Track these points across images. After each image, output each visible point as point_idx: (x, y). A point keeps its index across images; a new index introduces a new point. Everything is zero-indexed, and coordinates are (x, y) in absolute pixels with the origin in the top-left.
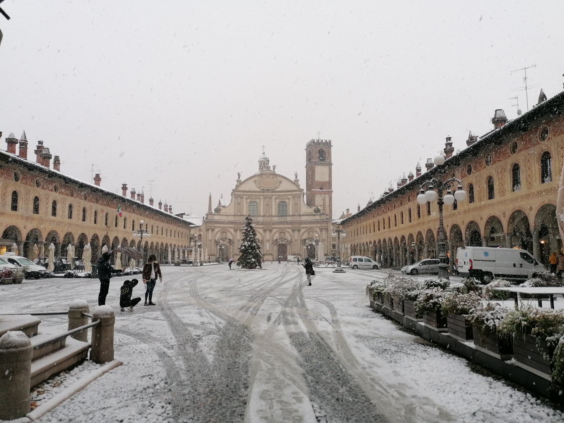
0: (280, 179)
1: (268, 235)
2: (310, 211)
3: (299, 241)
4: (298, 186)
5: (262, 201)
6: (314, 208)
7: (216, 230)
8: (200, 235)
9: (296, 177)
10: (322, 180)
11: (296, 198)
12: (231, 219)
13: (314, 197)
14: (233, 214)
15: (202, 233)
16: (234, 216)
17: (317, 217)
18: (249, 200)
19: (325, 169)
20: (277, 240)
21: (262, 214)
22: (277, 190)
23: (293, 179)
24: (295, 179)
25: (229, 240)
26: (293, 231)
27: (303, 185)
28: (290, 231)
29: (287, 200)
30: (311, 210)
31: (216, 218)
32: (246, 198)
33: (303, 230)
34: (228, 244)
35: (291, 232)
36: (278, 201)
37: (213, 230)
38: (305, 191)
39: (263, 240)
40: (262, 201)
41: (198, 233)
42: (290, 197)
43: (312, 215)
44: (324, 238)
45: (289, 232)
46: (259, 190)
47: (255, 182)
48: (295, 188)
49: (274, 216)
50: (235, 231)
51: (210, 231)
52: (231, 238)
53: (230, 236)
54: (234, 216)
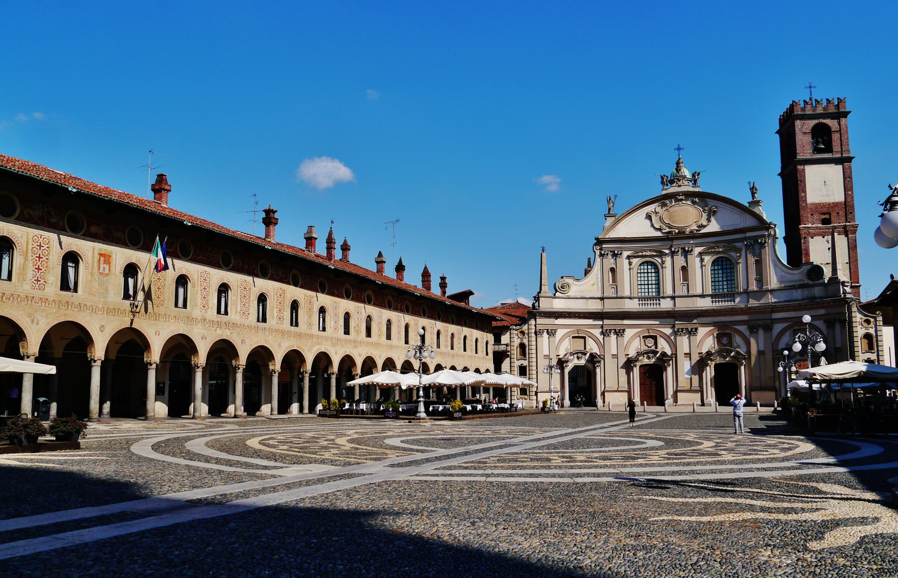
0: (711, 202)
1: (683, 342)
2: (797, 277)
3: (769, 355)
4: (759, 218)
5: (668, 260)
6: (805, 269)
7: (560, 333)
8: (522, 346)
9: (753, 194)
10: (832, 201)
11: (757, 247)
12: (595, 306)
13: (806, 243)
14: (599, 295)
15: (526, 341)
16: (602, 299)
17: (817, 291)
18: (636, 261)
19: (836, 171)
20: (709, 354)
21: (669, 291)
22: (704, 231)
23: (744, 199)
24: (750, 200)
25: (592, 356)
26: (753, 329)
27: (773, 211)
28: (743, 328)
29: (733, 254)
30: (797, 275)
31: (559, 305)
32: (628, 257)
33: (778, 328)
34: (590, 365)
35: (747, 333)
36: (708, 259)
37: (551, 333)
38: (780, 232)
39: (675, 355)
40: (668, 260)
41: (517, 342)
42: (738, 245)
43: (802, 286)
44: (838, 345)
45: (741, 334)
46: (659, 234)
47: (649, 217)
48: (750, 222)
49: (702, 296)
50: (602, 333)
51: (545, 334)
52: (596, 350)
53: (593, 347)
54: (602, 299)
